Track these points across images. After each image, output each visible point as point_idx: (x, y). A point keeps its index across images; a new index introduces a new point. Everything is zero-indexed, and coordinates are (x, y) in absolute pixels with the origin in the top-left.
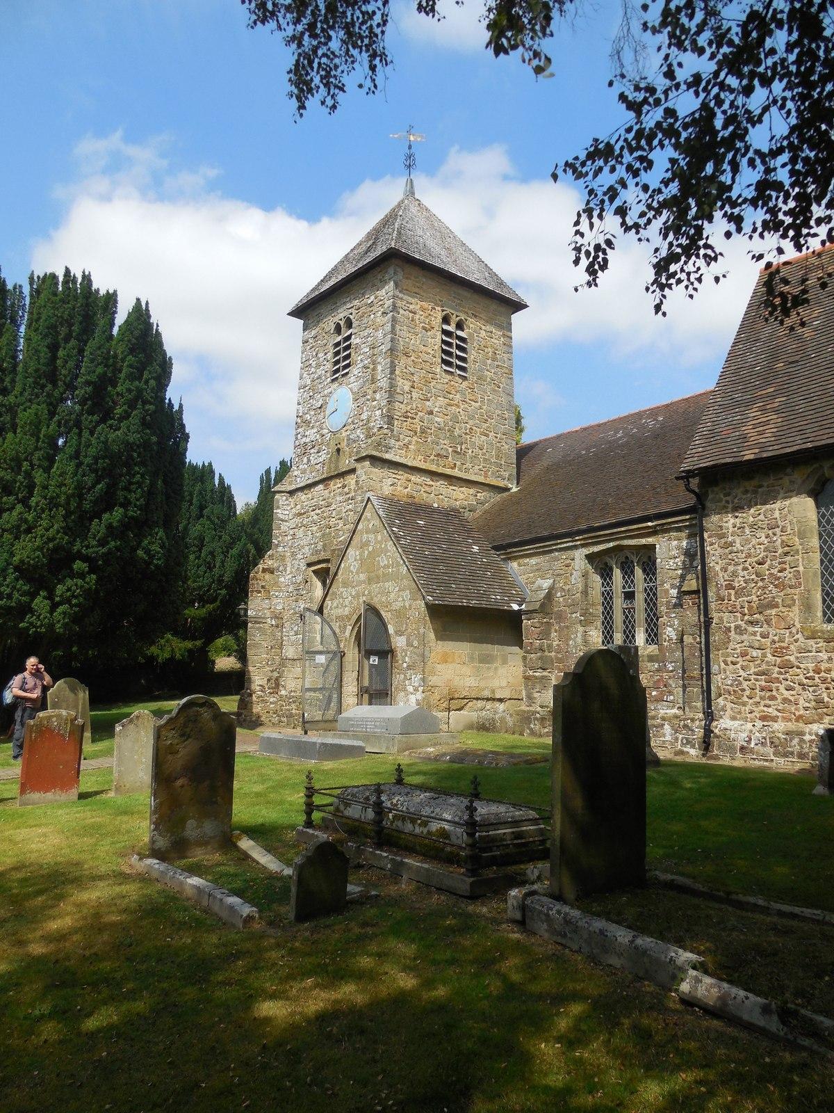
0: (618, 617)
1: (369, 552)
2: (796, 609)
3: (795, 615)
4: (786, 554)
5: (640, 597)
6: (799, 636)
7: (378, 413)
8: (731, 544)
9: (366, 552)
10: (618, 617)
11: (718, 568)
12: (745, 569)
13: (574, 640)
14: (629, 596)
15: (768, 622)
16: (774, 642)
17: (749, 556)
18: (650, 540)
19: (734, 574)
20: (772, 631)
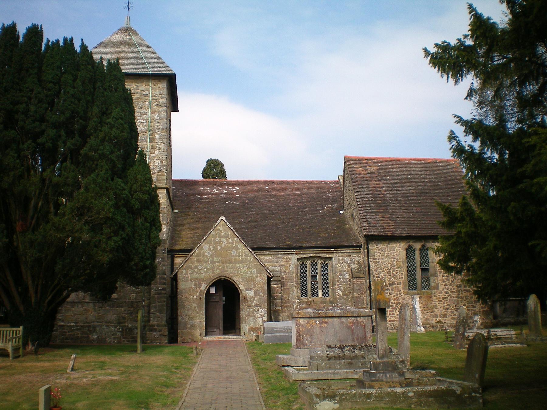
0: (309, 285)
1: (222, 248)
2: (401, 286)
3: (401, 287)
4: (398, 268)
5: (319, 278)
6: (403, 294)
7: (158, 162)
8: (378, 262)
9: (219, 248)
10: (309, 285)
11: (373, 270)
12: (383, 271)
13: (292, 294)
14: (314, 277)
15: (392, 290)
16: (394, 296)
17: (384, 267)
18: (330, 256)
19: (380, 272)
20: (393, 292)
